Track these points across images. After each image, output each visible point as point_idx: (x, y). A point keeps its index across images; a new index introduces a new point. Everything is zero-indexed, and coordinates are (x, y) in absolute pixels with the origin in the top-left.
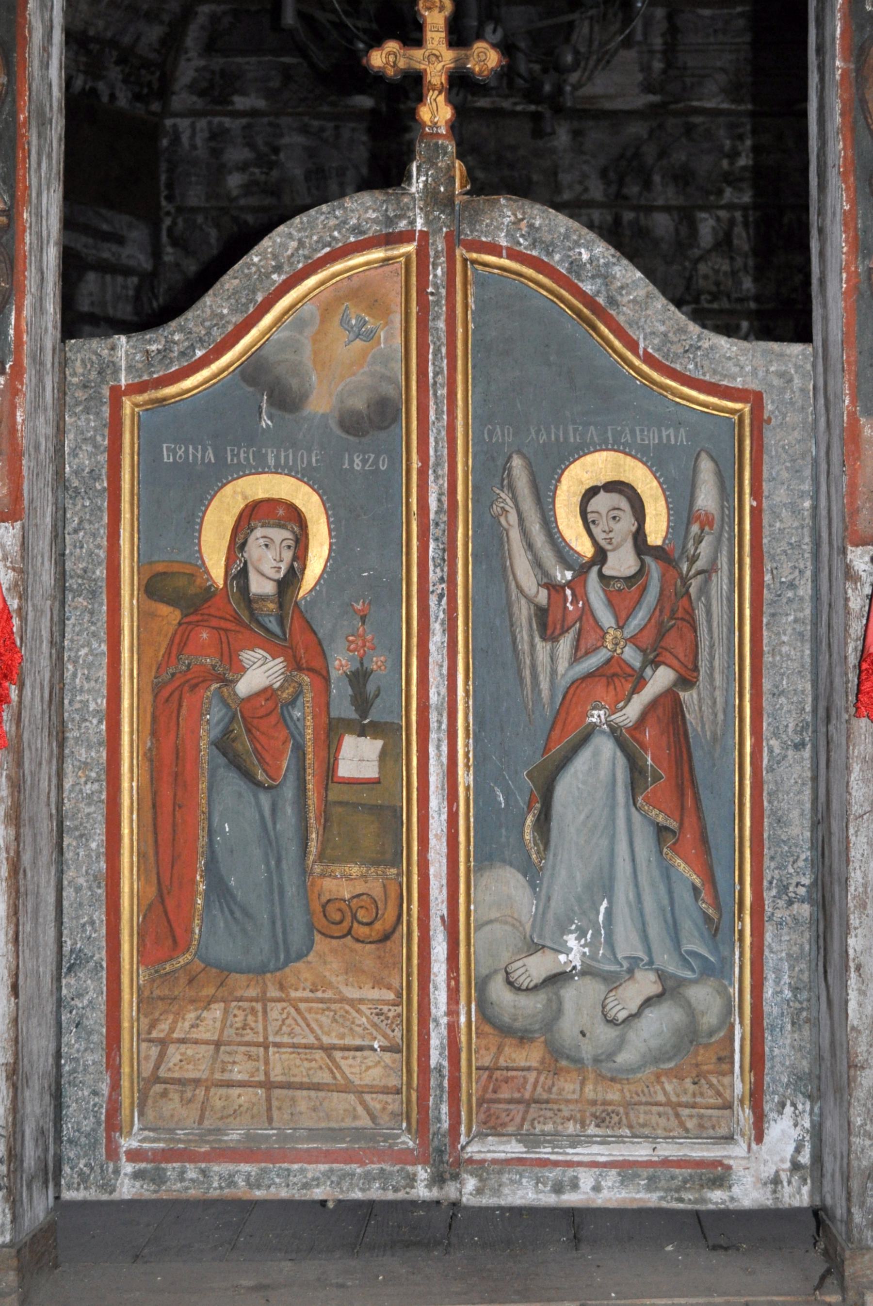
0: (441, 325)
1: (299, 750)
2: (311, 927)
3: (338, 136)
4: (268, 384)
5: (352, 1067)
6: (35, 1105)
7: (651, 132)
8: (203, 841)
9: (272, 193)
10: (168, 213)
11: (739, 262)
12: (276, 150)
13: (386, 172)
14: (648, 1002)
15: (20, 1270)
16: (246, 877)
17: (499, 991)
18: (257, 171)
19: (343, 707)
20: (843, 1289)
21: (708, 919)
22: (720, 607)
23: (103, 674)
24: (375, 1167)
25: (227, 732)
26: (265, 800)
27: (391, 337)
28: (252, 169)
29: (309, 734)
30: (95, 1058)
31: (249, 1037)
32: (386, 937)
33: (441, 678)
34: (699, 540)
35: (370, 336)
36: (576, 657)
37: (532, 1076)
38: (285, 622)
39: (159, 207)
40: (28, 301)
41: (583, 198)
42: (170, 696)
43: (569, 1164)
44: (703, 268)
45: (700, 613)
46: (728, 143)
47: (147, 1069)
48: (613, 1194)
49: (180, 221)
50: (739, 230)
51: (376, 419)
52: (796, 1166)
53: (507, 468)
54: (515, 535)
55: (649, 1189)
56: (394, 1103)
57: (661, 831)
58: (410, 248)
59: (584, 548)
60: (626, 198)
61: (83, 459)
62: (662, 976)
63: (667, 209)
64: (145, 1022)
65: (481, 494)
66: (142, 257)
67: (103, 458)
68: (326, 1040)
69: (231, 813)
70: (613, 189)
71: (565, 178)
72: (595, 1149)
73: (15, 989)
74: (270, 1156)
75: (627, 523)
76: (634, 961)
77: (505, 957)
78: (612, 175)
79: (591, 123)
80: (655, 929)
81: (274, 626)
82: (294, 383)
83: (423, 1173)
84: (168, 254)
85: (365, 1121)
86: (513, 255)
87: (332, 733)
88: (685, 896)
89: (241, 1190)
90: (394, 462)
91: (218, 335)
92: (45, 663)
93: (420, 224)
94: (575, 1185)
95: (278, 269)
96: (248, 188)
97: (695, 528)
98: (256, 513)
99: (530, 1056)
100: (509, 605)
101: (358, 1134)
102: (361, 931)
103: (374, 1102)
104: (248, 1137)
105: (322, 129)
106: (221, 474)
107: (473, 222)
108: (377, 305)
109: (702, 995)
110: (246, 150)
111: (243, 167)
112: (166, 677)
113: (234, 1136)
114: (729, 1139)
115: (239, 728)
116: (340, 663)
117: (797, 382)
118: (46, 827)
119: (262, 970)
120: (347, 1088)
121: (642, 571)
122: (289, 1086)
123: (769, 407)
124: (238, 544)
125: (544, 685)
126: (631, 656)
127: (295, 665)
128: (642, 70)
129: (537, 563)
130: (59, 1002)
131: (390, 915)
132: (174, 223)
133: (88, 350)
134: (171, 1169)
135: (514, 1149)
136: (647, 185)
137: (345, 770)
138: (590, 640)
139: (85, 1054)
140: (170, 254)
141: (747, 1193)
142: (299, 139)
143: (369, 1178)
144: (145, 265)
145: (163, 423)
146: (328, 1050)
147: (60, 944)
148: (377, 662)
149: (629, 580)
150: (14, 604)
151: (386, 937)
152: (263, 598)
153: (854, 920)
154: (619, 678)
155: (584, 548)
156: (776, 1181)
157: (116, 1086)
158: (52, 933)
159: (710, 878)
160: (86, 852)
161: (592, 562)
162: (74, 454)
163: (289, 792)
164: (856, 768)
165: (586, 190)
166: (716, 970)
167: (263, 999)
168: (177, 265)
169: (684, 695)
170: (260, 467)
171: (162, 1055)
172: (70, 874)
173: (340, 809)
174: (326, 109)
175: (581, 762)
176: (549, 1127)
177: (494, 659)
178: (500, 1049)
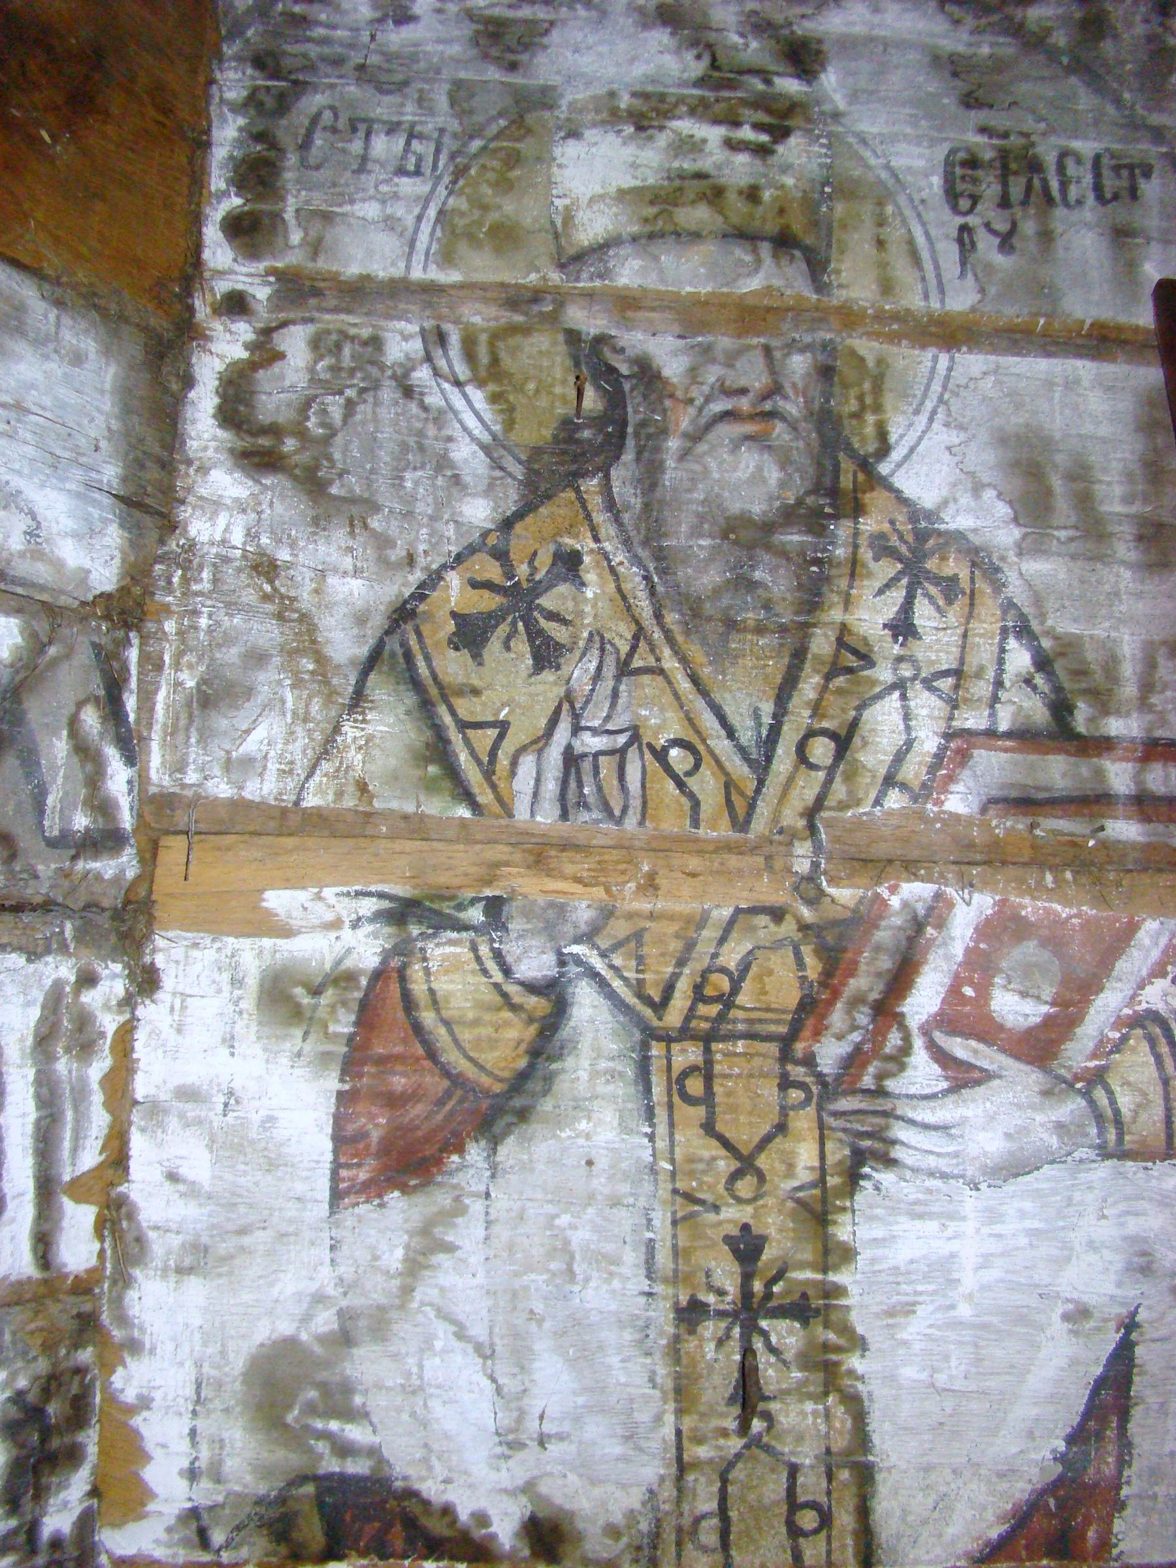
9: (784, 242)
10: (236, 305)
12: (803, 57)
18: (714, 134)
28: (685, 126)
39: (192, 268)
49: (295, 344)
66: (56, 507)
84: (215, 505)
96: (660, 212)
110: (661, 37)
132: (265, 352)
140: (223, 507)
144: (71, 554)
168: (265, 567)
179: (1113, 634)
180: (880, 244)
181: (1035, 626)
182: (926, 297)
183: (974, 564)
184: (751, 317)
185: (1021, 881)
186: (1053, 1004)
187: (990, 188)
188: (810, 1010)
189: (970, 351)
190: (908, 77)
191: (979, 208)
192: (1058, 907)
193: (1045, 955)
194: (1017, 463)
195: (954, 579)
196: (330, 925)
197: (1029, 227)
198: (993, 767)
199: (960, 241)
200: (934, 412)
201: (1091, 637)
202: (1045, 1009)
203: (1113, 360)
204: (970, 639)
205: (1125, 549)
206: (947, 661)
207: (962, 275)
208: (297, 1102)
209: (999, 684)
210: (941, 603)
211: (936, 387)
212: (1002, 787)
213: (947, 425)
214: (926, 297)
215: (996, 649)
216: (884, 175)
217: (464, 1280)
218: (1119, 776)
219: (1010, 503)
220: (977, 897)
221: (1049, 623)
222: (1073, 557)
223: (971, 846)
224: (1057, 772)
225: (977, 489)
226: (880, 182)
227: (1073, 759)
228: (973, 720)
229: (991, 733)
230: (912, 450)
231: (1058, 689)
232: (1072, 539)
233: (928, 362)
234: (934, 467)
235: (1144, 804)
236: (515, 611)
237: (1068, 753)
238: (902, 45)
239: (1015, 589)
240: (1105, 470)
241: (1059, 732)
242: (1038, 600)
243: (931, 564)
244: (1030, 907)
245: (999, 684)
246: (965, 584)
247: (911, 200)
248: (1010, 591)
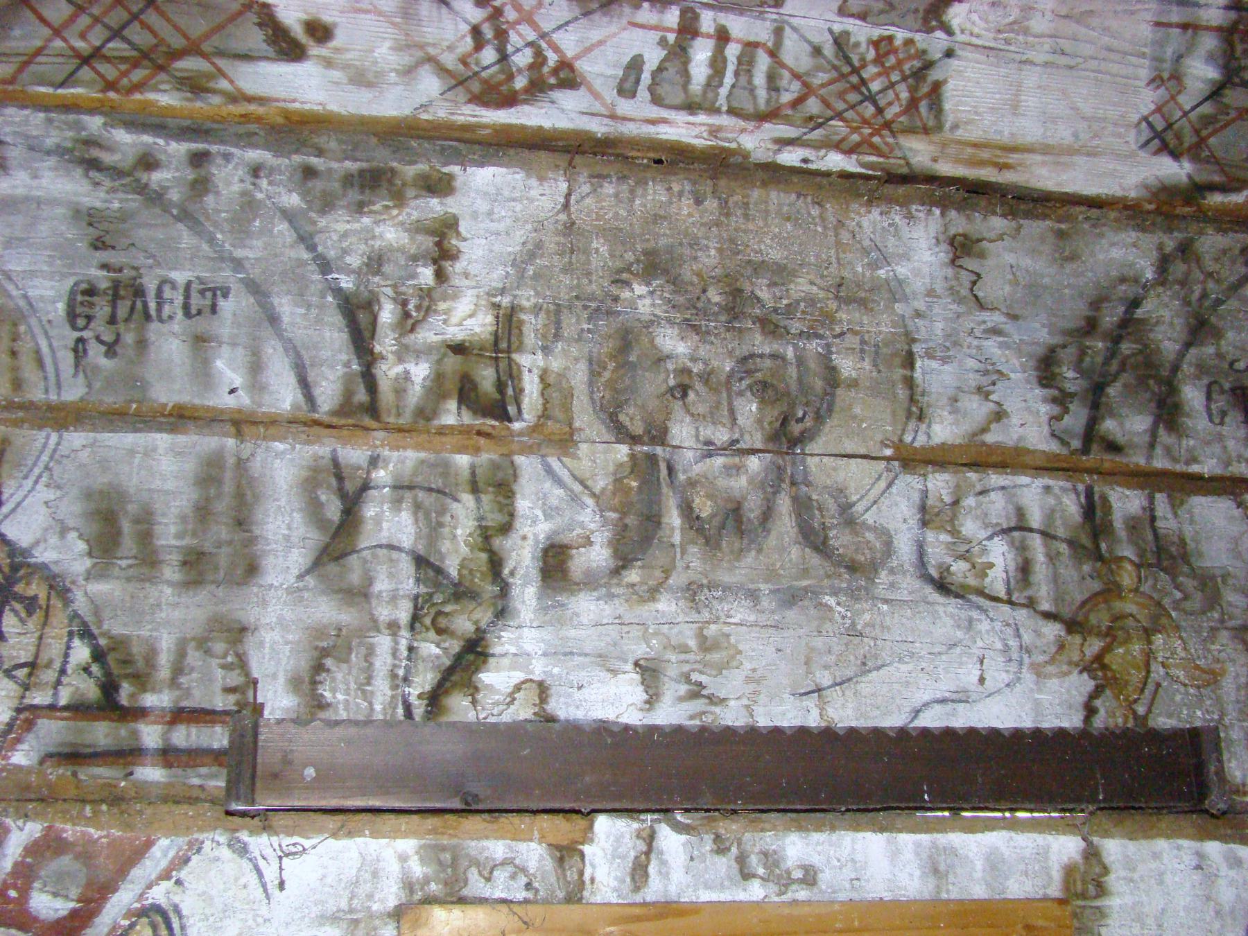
3: (201, 186)
7: (1163, 264)
41: (990, 438)
60: (1113, 447)
70: (1076, 418)
71: (935, 376)
78: (1069, 375)
79: (998, 223)
105: (148, 162)
128: (1156, 81)
136: (1168, 413)
142: (65, 186)
165: (999, 415)
174: (166, 98)
179: (154, 634)
180: (14, 354)
181: (96, 631)
182: (47, 391)
183: (51, 587)
185: (64, 812)
186: (79, 901)
187: (102, 310)
189: (76, 431)
190: (55, 226)
191: (92, 325)
192: (92, 830)
193: (77, 866)
194: (98, 512)
195: (35, 598)
197: (129, 338)
198: (51, 731)
199: (75, 350)
200: (40, 477)
201: (138, 636)
202: (72, 905)
203: (185, 433)
204: (44, 640)
205: (171, 572)
206: (25, 657)
207: (75, 375)
209: (63, 672)
210: (23, 615)
211: (45, 458)
212: (62, 744)
213: (47, 486)
214: (47, 391)
215: (64, 647)
216: (22, 303)
218: (151, 735)
219: (87, 541)
220: (30, 826)
221: (106, 627)
222: (128, 580)
223: (28, 788)
224: (101, 733)
225: (64, 531)
226: (18, 308)
227: (114, 724)
228: (39, 698)
229: (52, 707)
230: (18, 504)
231: (108, 674)
232: (130, 566)
233: (43, 439)
235: (168, 756)
237: (112, 720)
238: (53, 202)
239: (80, 603)
240: (164, 515)
241: (109, 705)
242: (97, 612)
243: (19, 588)
244: (70, 831)
245: (63, 672)
246: (42, 601)
247: (40, 321)
248: (75, 606)
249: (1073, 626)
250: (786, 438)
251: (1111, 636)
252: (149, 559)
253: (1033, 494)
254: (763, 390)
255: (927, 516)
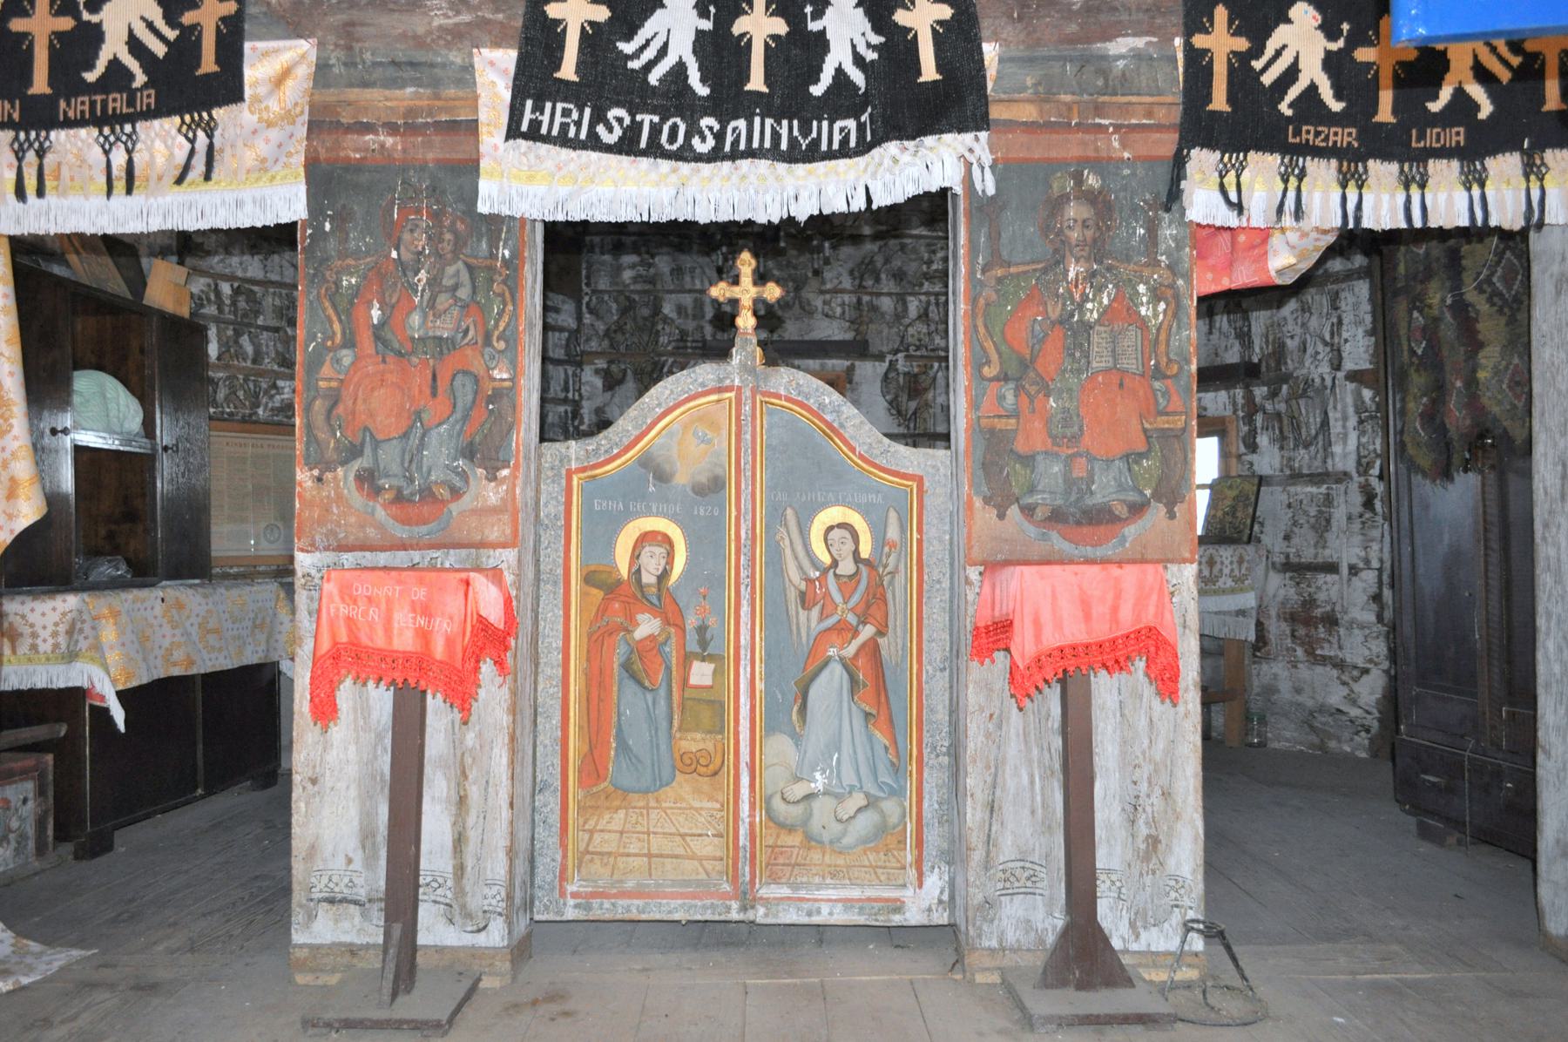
0: (748, 437)
1: (668, 669)
2: (674, 767)
4: (655, 470)
5: (696, 845)
6: (521, 867)
8: (615, 719)
11: (933, 327)
13: (721, 352)
14: (859, 810)
15: (512, 962)
16: (638, 739)
17: (777, 803)
19: (692, 645)
20: (964, 971)
21: (893, 764)
22: (899, 593)
23: (561, 628)
24: (708, 902)
25: (629, 659)
26: (649, 697)
27: (722, 442)
29: (674, 661)
30: (554, 840)
31: (639, 828)
32: (716, 773)
33: (746, 632)
34: (888, 556)
35: (709, 442)
36: (821, 620)
37: (795, 851)
38: (662, 600)
39: (581, 290)
40: (523, 426)
42: (597, 640)
43: (816, 900)
44: (911, 330)
45: (889, 596)
46: (926, 256)
47: (582, 847)
48: (840, 917)
50: (932, 308)
51: (712, 487)
52: (940, 902)
53: (783, 515)
54: (788, 552)
55: (860, 914)
56: (719, 866)
57: (867, 715)
58: (732, 395)
59: (827, 560)
61: (551, 508)
62: (867, 795)
63: (889, 294)
64: (581, 821)
65: (768, 527)
67: (562, 508)
68: (682, 831)
69: (630, 704)
72: (831, 892)
73: (511, 805)
74: (649, 896)
75: (850, 546)
76: (852, 787)
77: (782, 785)
80: (864, 770)
81: (655, 601)
82: (667, 467)
83: (735, 905)
85: (703, 876)
86: (788, 399)
87: (686, 660)
88: (880, 751)
89: (634, 915)
90: (722, 509)
91: (626, 442)
92: (529, 622)
93: (737, 382)
94: (819, 912)
95: (659, 405)
96: (635, 280)
97: (886, 549)
98: (645, 538)
99: (795, 839)
100: (785, 590)
101: (699, 883)
102: (702, 770)
103: (708, 865)
104: (638, 885)
106: (627, 516)
107: (766, 379)
108: (714, 426)
109: (890, 807)
111: (633, 266)
112: (594, 628)
113: (630, 885)
114: (904, 886)
115: (635, 657)
116: (691, 621)
117: (942, 470)
118: (528, 712)
119: (647, 791)
120: (692, 858)
121: (857, 572)
122: (661, 856)
123: (927, 484)
124: (635, 556)
125: (804, 635)
126: (852, 619)
127: (667, 622)
129: (800, 568)
130: (534, 810)
131: (718, 761)
133: (552, 450)
134: (595, 902)
135: (785, 891)
136: (878, 280)
137: (693, 681)
138: (828, 610)
139: (548, 838)
140: (588, 318)
141: (913, 916)
143: (705, 907)
145: (595, 486)
146: (683, 836)
147: (534, 778)
148: (712, 621)
149: (851, 577)
150: (513, 593)
151: (716, 773)
152: (649, 585)
153: (970, 769)
154: (845, 631)
155: (827, 560)
156: (930, 910)
157: (565, 856)
158: (530, 769)
159: (895, 742)
160: (549, 726)
161: (830, 567)
162: (546, 505)
163: (662, 692)
164: (971, 686)
166: (896, 793)
167: (647, 808)
169: (880, 641)
170: (648, 513)
171: (590, 839)
172: (540, 738)
173: (689, 703)
175: (825, 675)
176: (805, 879)
177: (776, 621)
178: (778, 836)
184: (645, 292)
188: (653, 371)
196: (601, 364)
208: (599, 382)
217: (616, 400)
234: (668, 309)
236: (620, 329)
249: (852, 322)
250: (798, 289)
251: (861, 324)
252: (687, 316)
253: (846, 298)
254: (794, 281)
255: (825, 303)
